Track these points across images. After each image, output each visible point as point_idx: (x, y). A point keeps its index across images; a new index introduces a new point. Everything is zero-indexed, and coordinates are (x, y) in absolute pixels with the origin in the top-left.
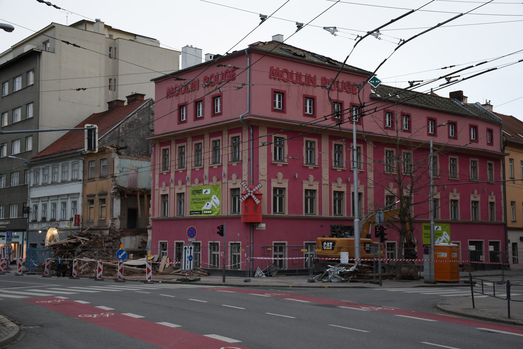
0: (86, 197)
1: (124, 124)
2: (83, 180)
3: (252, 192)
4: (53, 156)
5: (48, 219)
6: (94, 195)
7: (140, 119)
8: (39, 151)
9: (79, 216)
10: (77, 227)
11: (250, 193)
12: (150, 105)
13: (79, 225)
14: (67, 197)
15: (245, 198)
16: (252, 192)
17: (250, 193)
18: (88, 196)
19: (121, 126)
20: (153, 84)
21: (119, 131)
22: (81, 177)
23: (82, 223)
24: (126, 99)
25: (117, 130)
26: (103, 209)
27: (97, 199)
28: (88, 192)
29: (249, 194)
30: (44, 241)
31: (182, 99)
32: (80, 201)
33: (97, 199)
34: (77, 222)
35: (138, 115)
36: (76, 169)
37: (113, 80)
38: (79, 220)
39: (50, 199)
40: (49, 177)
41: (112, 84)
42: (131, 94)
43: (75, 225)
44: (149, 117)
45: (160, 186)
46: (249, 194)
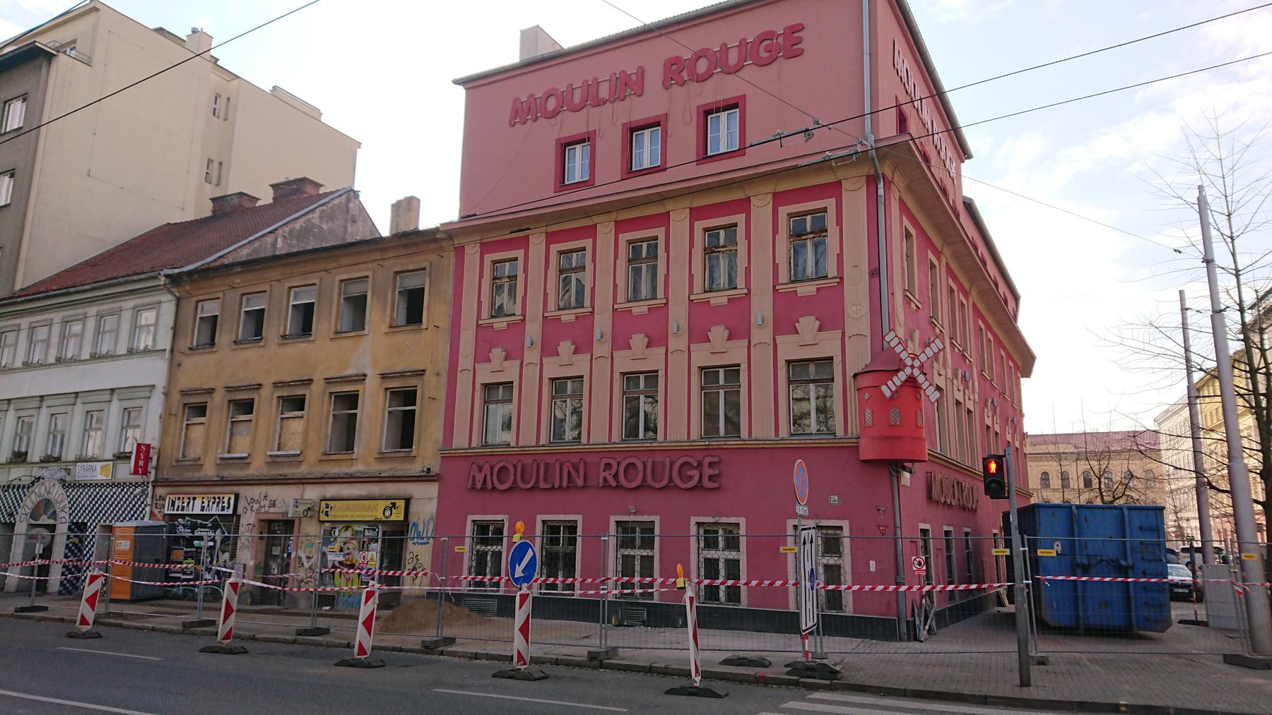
0: (176, 396)
1: (287, 229)
2: (172, 351)
3: (917, 363)
4: (72, 290)
5: (36, 455)
6: (210, 391)
7: (325, 227)
8: (18, 287)
9: (148, 446)
10: (138, 478)
11: (912, 367)
12: (348, 200)
13: (145, 472)
14: (107, 397)
15: (898, 383)
16: (917, 363)
17: (912, 367)
18: (184, 393)
19: (280, 232)
20: (461, 92)
21: (274, 245)
22: (165, 342)
23: (157, 468)
24: (271, 192)
25: (269, 239)
26: (242, 427)
27: (217, 402)
28: (185, 382)
29: (908, 371)
30: (11, 515)
31: (573, 124)
32: (155, 406)
33: (217, 402)
34: (141, 463)
35: (321, 218)
36: (155, 318)
37: (216, 165)
38: (148, 459)
39: (45, 403)
40: (48, 347)
41: (214, 169)
42: (283, 180)
43: (136, 472)
44: (345, 228)
45: (482, 356)
46: (908, 371)
